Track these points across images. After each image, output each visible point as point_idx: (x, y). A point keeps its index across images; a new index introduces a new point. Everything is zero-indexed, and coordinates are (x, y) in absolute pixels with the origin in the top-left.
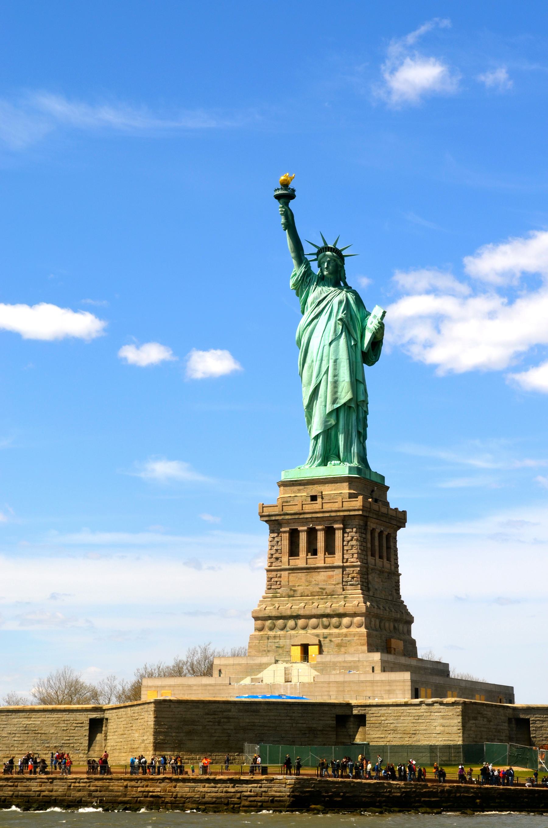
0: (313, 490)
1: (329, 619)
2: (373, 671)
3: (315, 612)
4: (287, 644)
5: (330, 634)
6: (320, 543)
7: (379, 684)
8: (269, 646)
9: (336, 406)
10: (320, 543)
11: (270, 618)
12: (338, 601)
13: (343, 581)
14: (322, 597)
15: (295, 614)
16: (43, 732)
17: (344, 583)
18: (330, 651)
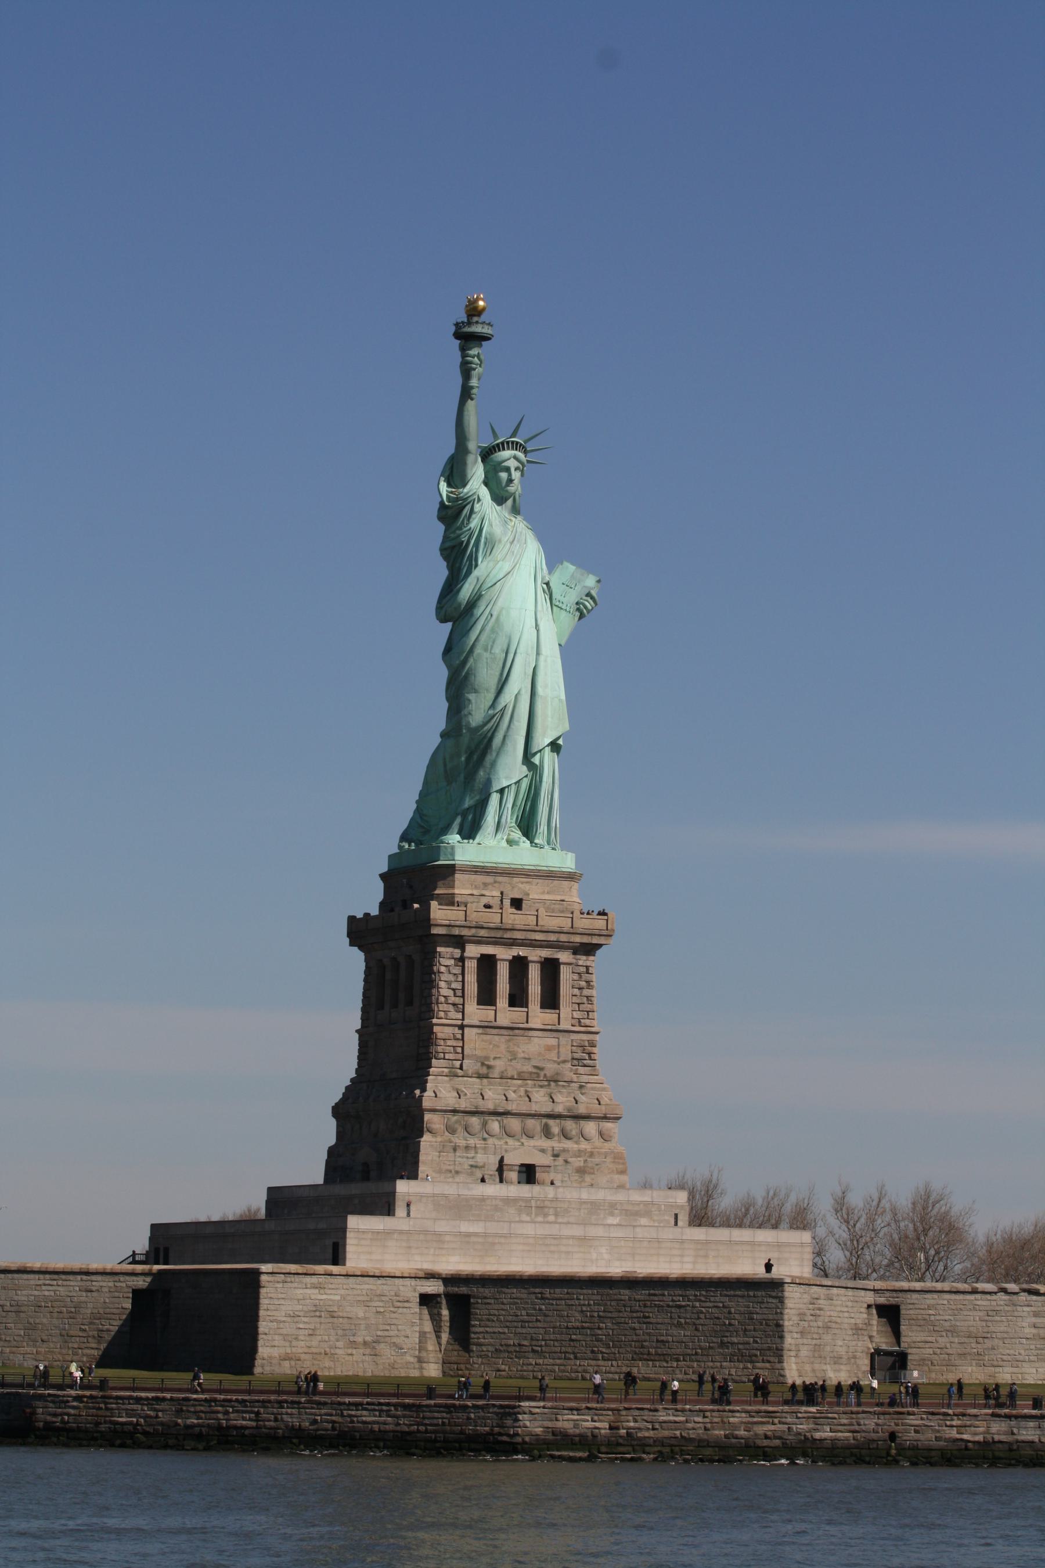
0: (516, 889)
1: (558, 1121)
2: (676, 1224)
3: (535, 1108)
4: (490, 1162)
5: (564, 1150)
6: (533, 987)
7: (763, 1248)
8: (457, 1163)
9: (548, 741)
10: (533, 987)
11: (455, 1111)
12: (569, 1093)
13: (573, 1059)
14: (541, 1083)
15: (501, 1110)
16: (345, 1315)
17: (576, 1062)
18: (566, 1179)
